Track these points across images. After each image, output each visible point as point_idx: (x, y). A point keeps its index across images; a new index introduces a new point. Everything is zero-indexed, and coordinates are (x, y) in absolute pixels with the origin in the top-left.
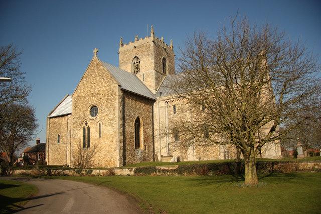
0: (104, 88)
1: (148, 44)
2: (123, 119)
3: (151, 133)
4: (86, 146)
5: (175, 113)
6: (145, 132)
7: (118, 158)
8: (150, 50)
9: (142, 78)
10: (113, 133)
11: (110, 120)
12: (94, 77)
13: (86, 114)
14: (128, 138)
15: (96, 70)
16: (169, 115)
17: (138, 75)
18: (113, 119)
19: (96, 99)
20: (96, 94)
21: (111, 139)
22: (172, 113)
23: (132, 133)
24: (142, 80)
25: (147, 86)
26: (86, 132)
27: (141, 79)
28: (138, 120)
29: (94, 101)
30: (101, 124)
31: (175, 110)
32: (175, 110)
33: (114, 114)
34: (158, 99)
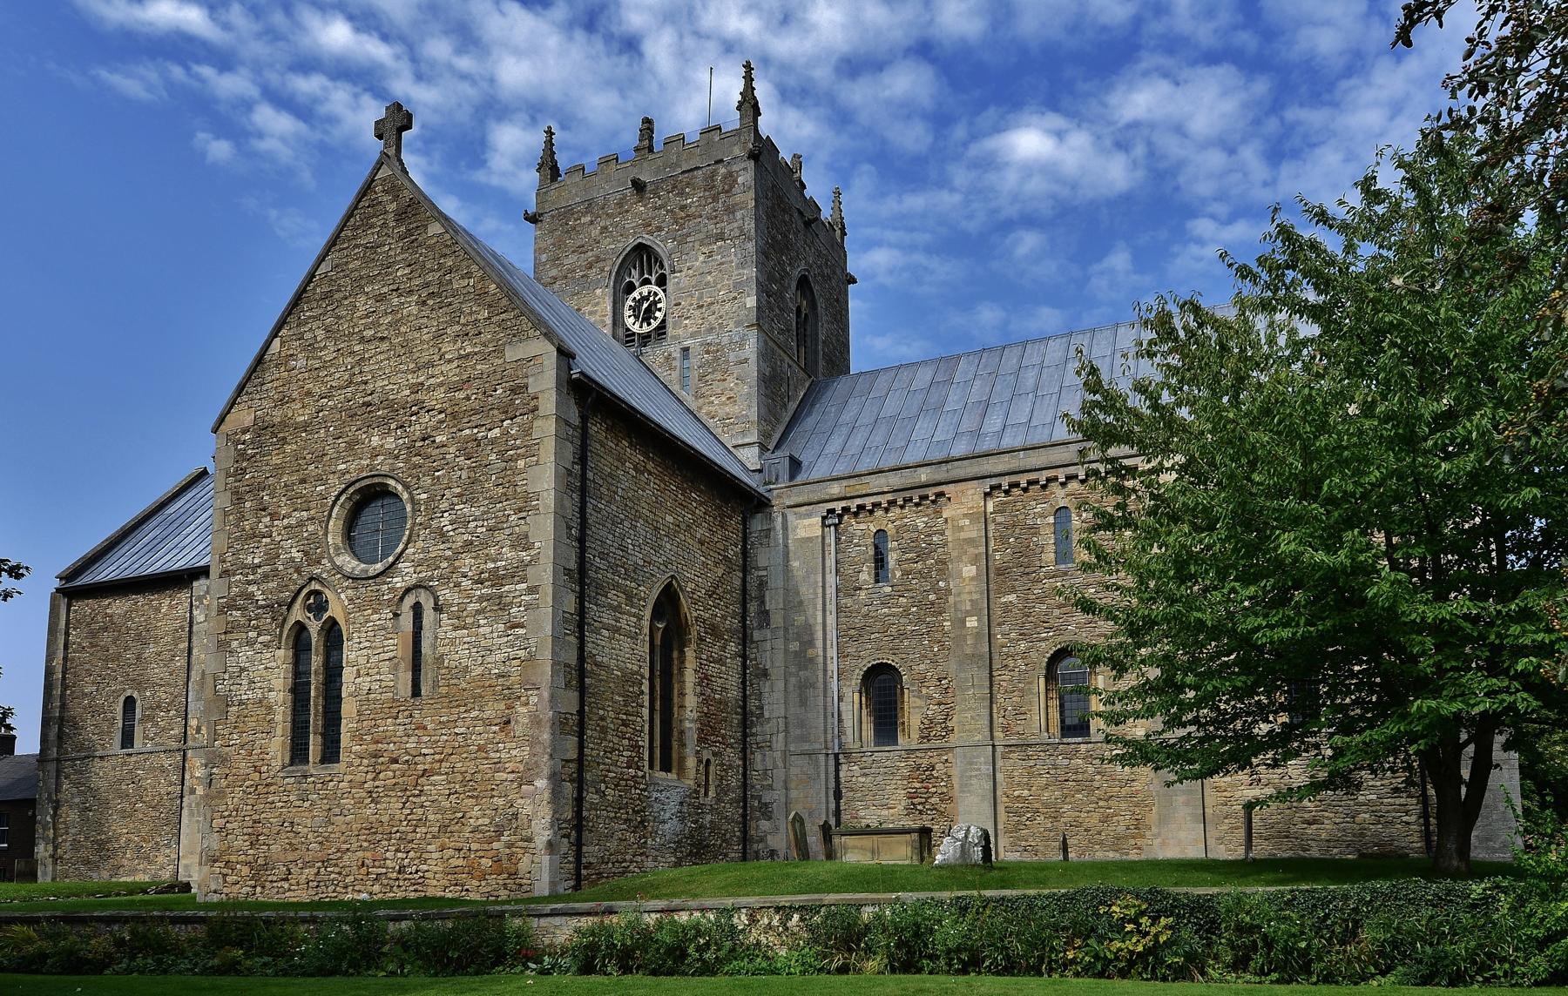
1: (722, 171)
2: (580, 578)
3: (734, 693)
4: (315, 744)
6: (704, 680)
7: (542, 832)
8: (730, 210)
9: (675, 374)
10: (514, 669)
11: (497, 579)
13: (321, 543)
14: (607, 710)
17: (654, 355)
18: (517, 573)
19: (390, 443)
21: (493, 710)
22: (866, 576)
23: (629, 678)
24: (675, 388)
26: (316, 661)
27: (672, 378)
28: (668, 603)
29: (380, 450)
30: (428, 616)
31: (880, 561)
32: (880, 561)
33: (522, 542)
34: (782, 496)
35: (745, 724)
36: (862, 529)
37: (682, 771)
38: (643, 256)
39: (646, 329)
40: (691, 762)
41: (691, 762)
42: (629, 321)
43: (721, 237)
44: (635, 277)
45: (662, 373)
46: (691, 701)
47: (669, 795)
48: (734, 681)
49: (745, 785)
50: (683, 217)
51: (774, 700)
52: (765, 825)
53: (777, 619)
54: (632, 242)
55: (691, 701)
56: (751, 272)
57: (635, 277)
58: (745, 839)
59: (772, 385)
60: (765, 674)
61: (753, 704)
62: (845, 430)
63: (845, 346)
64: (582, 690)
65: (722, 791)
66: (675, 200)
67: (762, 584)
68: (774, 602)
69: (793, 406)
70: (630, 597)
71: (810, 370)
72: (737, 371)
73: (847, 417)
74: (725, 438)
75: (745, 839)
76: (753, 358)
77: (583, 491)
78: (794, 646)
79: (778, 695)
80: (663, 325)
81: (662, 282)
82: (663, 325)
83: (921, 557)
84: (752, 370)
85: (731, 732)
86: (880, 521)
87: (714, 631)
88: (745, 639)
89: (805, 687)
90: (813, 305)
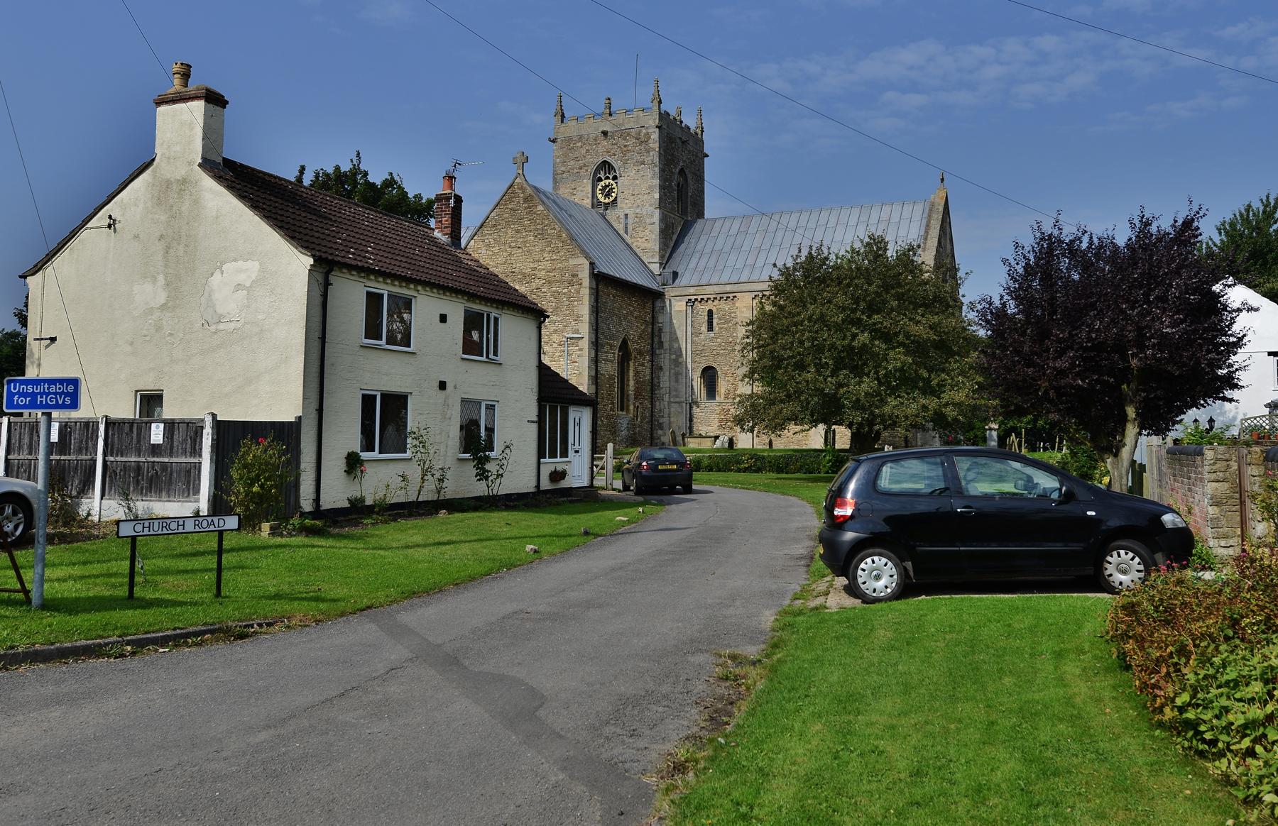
0: (548, 265)
2: (596, 345)
3: (648, 377)
5: (710, 328)
6: (637, 374)
12: (518, 231)
15: (522, 211)
16: (696, 333)
17: (611, 215)
20: (524, 275)
22: (704, 328)
23: (611, 378)
24: (622, 232)
25: (637, 251)
28: (624, 346)
34: (669, 292)
35: (652, 390)
36: (703, 309)
37: (628, 411)
38: (606, 166)
39: (607, 201)
40: (632, 407)
41: (632, 407)
42: (600, 196)
43: (643, 163)
44: (602, 175)
45: (615, 225)
46: (632, 383)
47: (624, 421)
48: (648, 372)
49: (652, 415)
50: (625, 151)
51: (665, 380)
52: (660, 432)
53: (666, 345)
54: (601, 159)
55: (632, 383)
56: (657, 182)
57: (602, 175)
58: (652, 438)
59: (665, 232)
60: (661, 368)
61: (656, 380)
62: (698, 255)
63: (703, 192)
64: (597, 384)
65: (643, 418)
66: (621, 142)
67: (660, 330)
68: (665, 338)
69: (675, 237)
70: (611, 346)
71: (684, 212)
72: (650, 227)
73: (699, 247)
74: (644, 258)
75: (652, 438)
76: (657, 223)
77: (597, 313)
78: (674, 357)
79: (666, 378)
80: (615, 200)
81: (615, 178)
82: (615, 200)
83: (726, 322)
84: (657, 228)
85: (647, 394)
86: (709, 306)
87: (641, 353)
88: (653, 354)
89: (677, 374)
90: (686, 180)
